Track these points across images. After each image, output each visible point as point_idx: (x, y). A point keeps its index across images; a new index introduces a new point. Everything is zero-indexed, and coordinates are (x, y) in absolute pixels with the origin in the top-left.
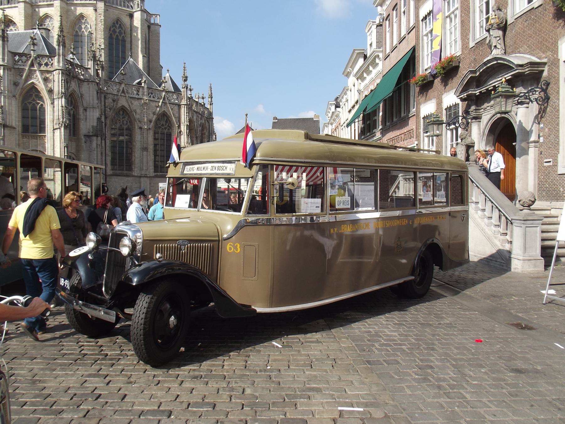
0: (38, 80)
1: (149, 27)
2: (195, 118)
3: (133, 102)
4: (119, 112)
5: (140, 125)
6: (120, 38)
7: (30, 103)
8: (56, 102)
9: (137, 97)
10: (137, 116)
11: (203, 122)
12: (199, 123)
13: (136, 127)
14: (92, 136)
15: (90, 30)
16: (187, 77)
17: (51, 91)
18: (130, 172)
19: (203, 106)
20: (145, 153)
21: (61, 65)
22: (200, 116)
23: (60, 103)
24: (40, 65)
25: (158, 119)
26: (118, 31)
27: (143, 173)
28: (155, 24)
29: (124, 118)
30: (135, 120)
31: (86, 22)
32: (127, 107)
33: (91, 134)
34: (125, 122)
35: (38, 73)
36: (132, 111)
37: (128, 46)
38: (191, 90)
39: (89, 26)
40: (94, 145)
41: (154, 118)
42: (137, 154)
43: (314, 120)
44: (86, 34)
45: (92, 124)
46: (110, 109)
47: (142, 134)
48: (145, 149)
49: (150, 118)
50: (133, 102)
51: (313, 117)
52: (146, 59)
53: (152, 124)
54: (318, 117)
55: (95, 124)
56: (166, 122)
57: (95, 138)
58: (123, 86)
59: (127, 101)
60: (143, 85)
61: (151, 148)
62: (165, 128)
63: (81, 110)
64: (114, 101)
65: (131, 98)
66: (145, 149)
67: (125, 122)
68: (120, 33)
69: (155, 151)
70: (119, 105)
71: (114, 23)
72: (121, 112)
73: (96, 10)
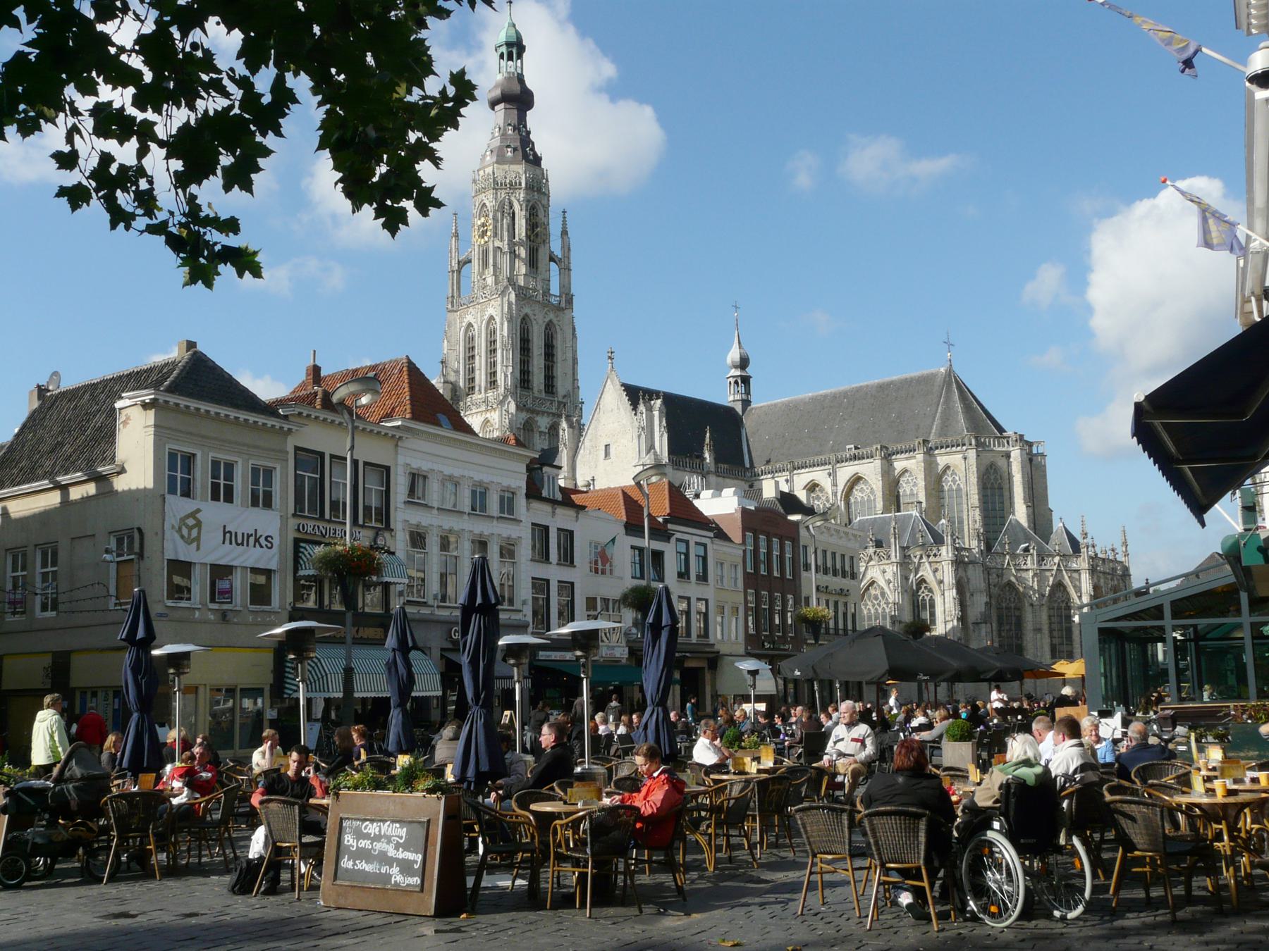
0: (926, 572)
1: (1031, 460)
2: (1102, 581)
4: (1005, 587)
6: (996, 486)
8: (946, 593)
9: (1025, 567)
11: (1116, 582)
12: (1110, 586)
13: (1027, 604)
14: (981, 623)
15: (958, 482)
16: (1086, 534)
17: (941, 582)
19: (1115, 561)
20: (1039, 636)
21: (950, 555)
22: (1109, 577)
23: (951, 594)
24: (929, 556)
26: (992, 477)
28: (1038, 454)
31: (954, 473)
33: (979, 621)
34: (1012, 600)
35: (927, 564)
37: (1006, 494)
38: (1093, 547)
39: (957, 478)
40: (983, 633)
42: (1029, 637)
44: (954, 488)
45: (979, 610)
46: (994, 586)
48: (1038, 630)
52: (1031, 510)
55: (983, 610)
57: (984, 625)
60: (1031, 551)
61: (1046, 628)
62: (1063, 601)
63: (968, 595)
64: (997, 575)
66: (1038, 630)
67: (1012, 600)
68: (996, 479)
69: (1051, 631)
70: (1005, 580)
71: (987, 469)
72: (1007, 588)
73: (965, 458)
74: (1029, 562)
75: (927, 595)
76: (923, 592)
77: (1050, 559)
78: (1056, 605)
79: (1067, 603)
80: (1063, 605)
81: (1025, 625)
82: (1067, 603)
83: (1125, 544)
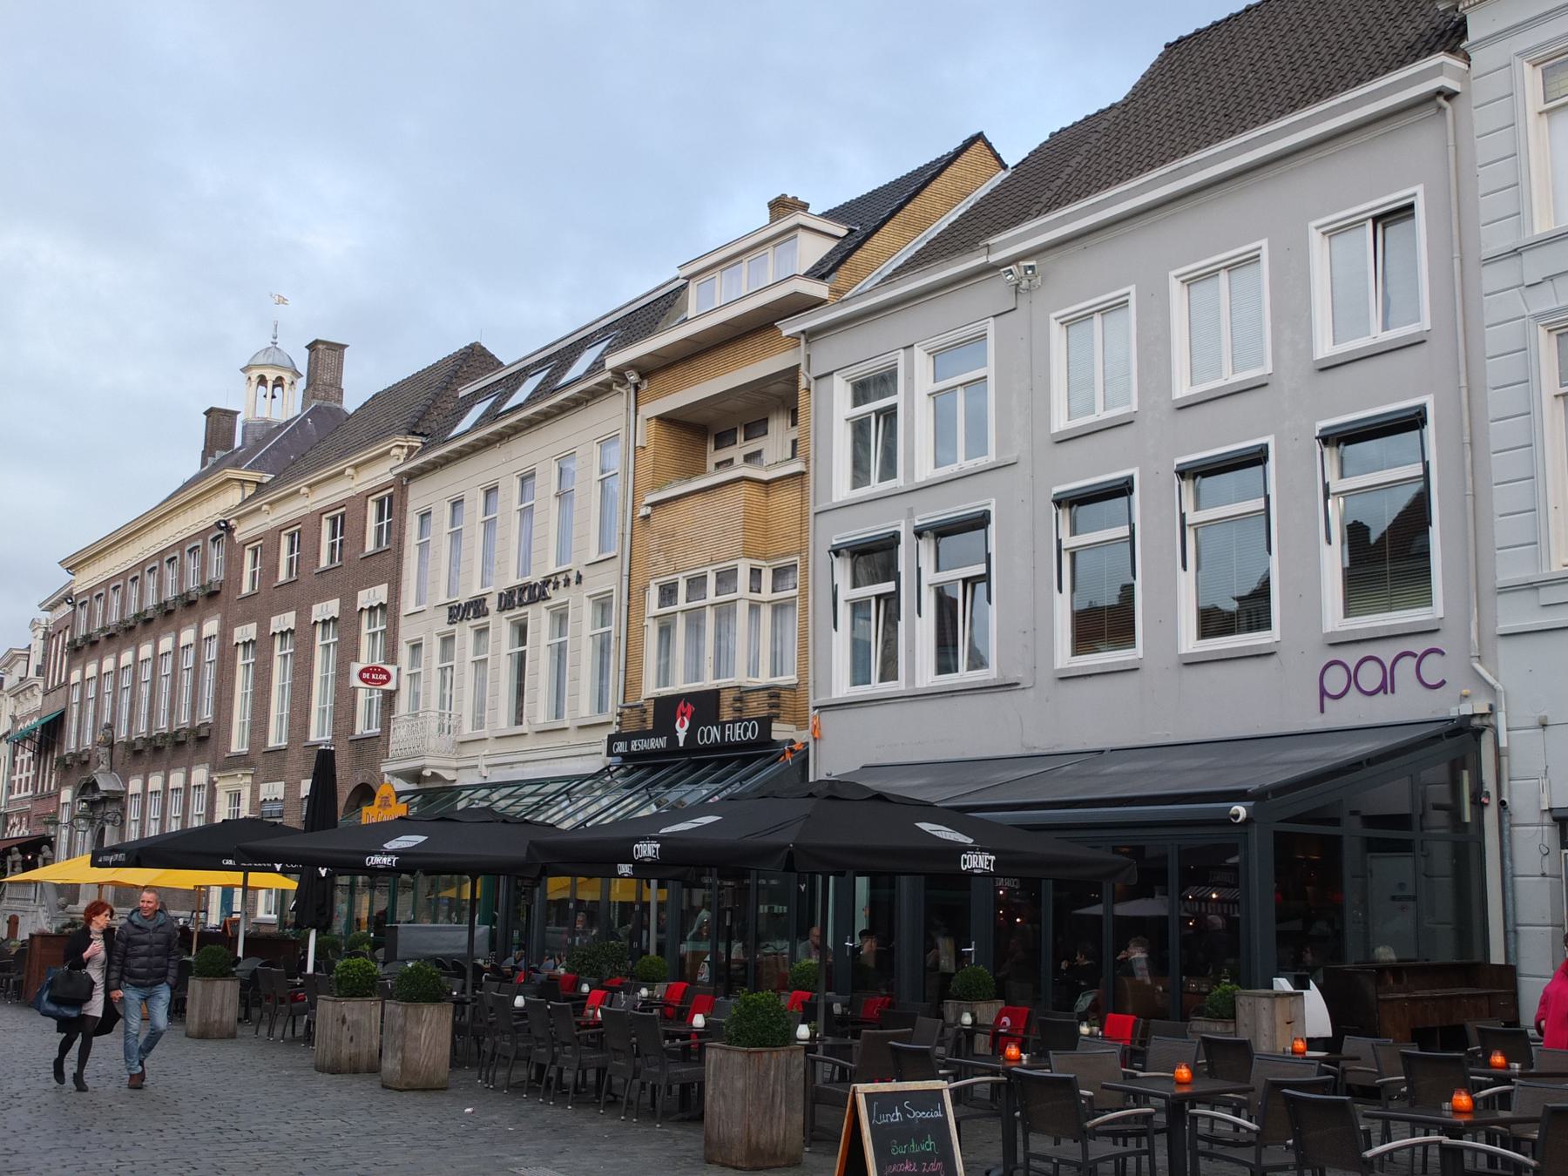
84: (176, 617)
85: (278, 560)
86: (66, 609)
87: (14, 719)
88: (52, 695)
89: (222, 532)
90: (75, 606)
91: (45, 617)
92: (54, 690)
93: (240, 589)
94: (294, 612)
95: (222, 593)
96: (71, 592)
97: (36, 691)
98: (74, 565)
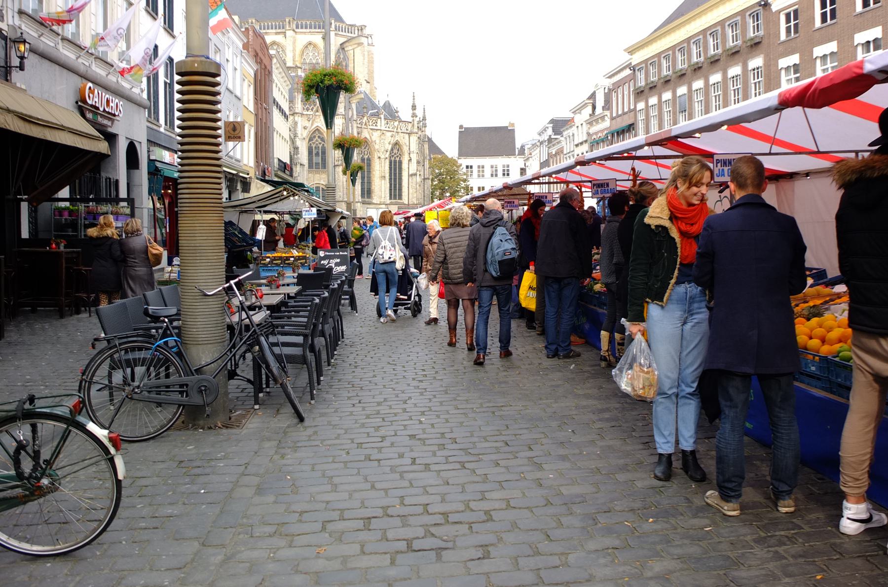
3: (374, 133)
5: (379, 155)
7: (314, 143)
9: (376, 128)
10: (377, 147)
13: (376, 157)
18: (369, 200)
25: (392, 150)
27: (382, 200)
29: (364, 148)
30: (375, 150)
32: (368, 138)
34: (366, 153)
36: (372, 142)
41: (389, 147)
43: (509, 128)
47: (380, 163)
49: (386, 148)
50: (374, 133)
51: (507, 125)
53: (388, 153)
54: (513, 125)
56: (398, 150)
58: (365, 118)
59: (368, 132)
62: (397, 156)
65: (371, 129)
67: (366, 153)
70: (363, 137)
74: (379, 124)
75: (320, 143)
76: (317, 141)
77: (392, 123)
78: (393, 159)
79: (400, 158)
80: (398, 159)
81: (374, 173)
82: (400, 158)
83: (424, 119)
84: (721, 63)
85: (814, 14)
86: (628, 72)
87: (588, 134)
88: (618, 119)
89: (761, 8)
90: (634, 71)
91: (609, 83)
92: (615, 118)
93: (779, 37)
94: (836, 42)
95: (763, 42)
96: (631, 64)
97: (606, 118)
98: (631, 51)
